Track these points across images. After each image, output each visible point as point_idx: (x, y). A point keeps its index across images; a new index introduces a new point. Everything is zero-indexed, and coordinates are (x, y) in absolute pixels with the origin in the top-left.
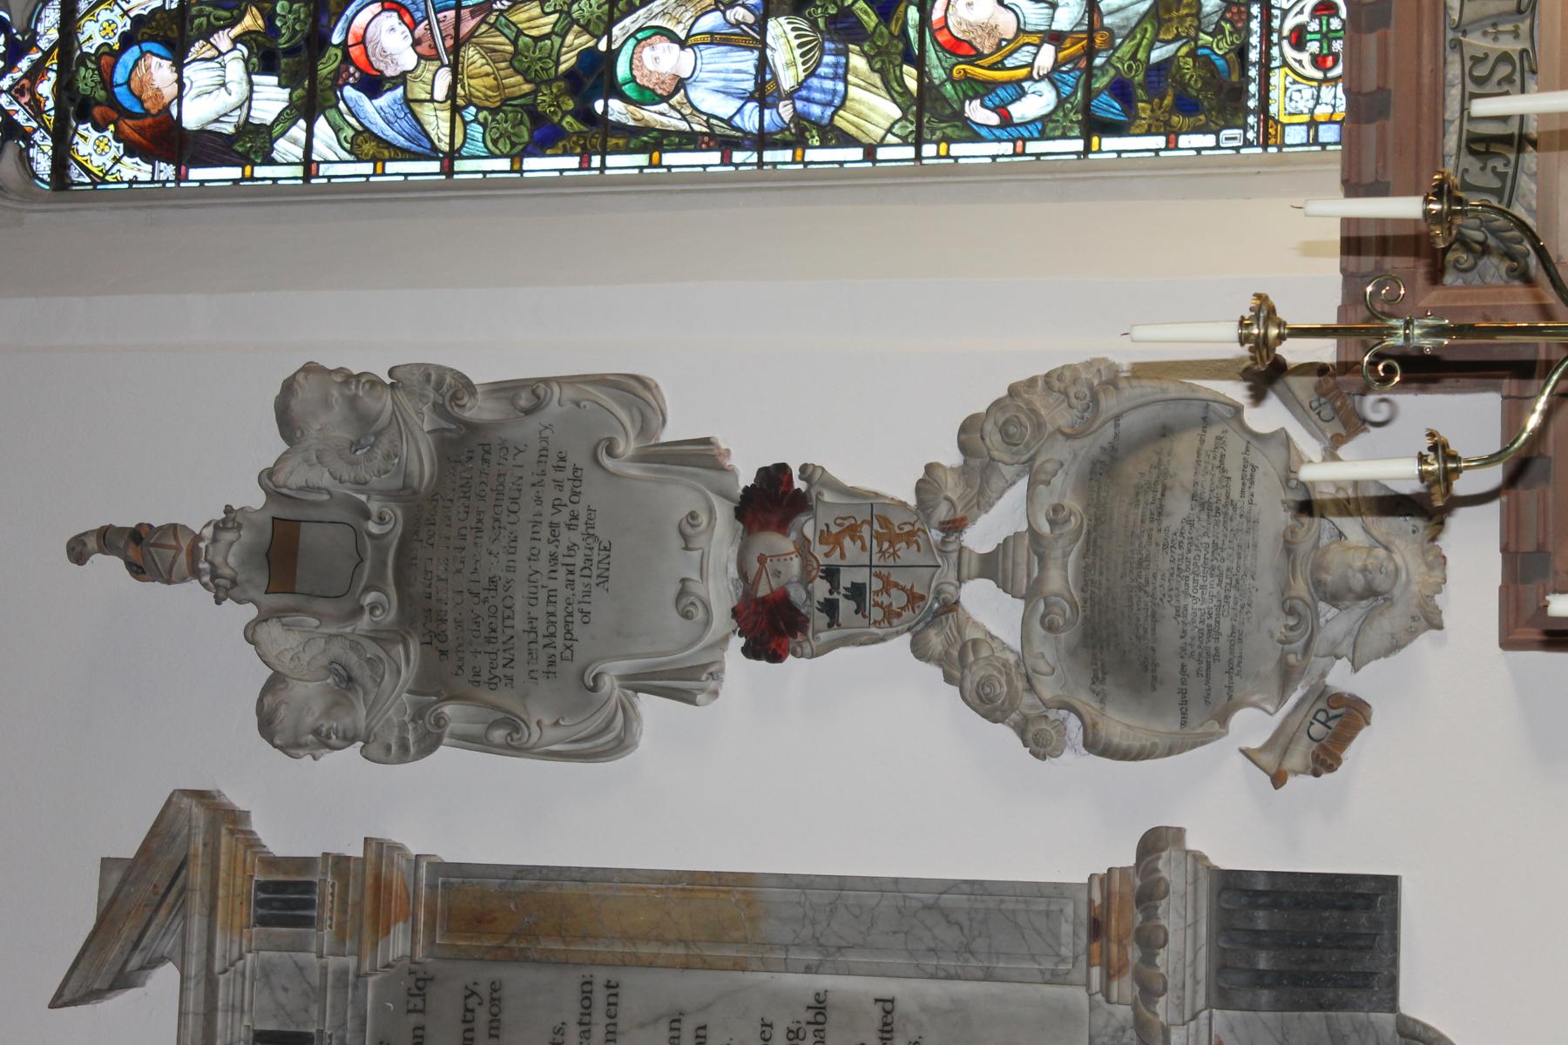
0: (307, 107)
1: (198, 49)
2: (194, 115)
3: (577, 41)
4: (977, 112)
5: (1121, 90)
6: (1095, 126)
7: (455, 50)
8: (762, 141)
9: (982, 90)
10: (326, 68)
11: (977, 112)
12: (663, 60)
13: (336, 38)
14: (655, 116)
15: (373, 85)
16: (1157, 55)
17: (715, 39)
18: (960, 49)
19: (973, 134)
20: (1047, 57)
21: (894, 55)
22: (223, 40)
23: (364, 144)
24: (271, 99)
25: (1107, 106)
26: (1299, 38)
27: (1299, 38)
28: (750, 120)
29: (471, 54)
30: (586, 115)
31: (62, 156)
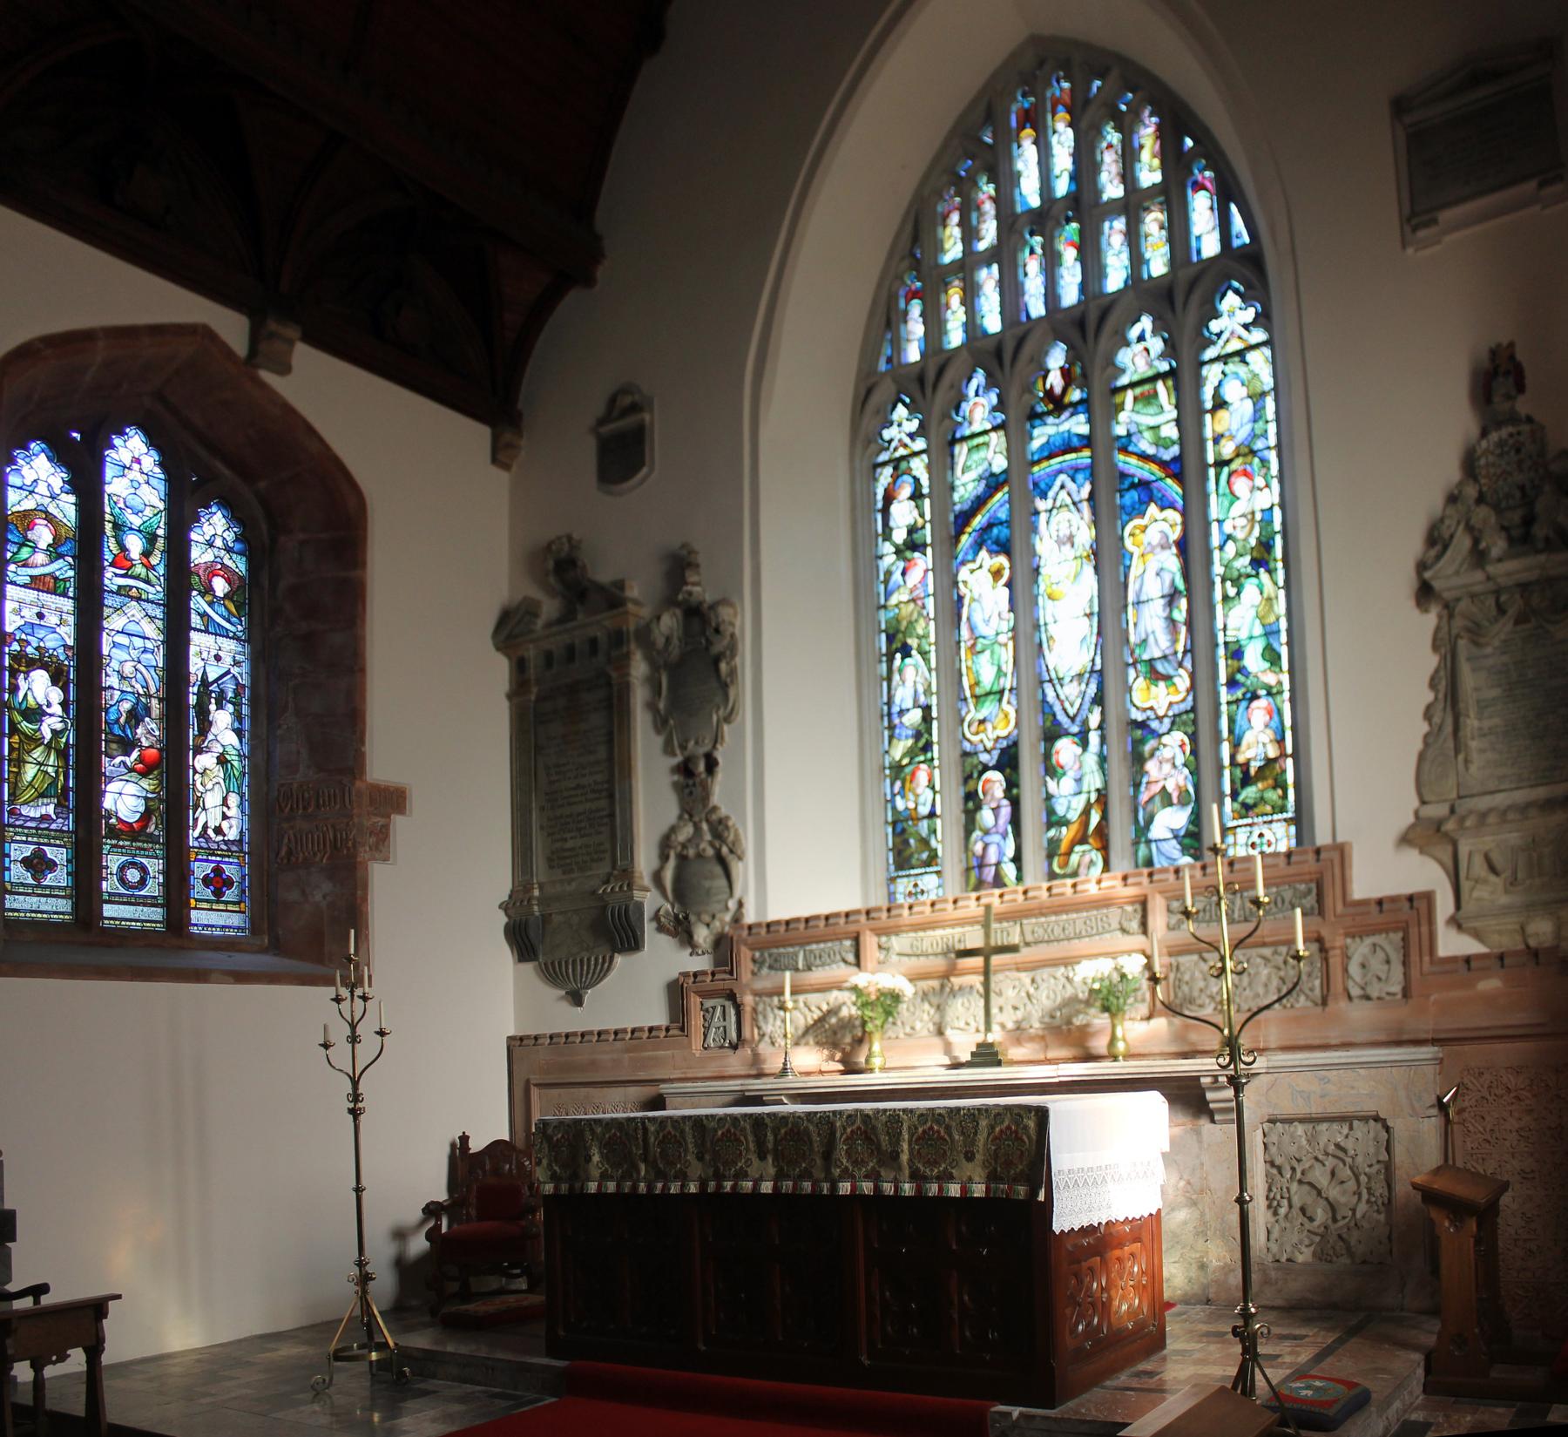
0: (899, 552)
1: (912, 503)
2: (894, 508)
3: (913, 642)
4: (898, 784)
5: (904, 831)
6: (894, 823)
7: (913, 600)
8: (890, 714)
9: (903, 787)
10: (908, 554)
11: (898, 784)
12: (910, 673)
13: (916, 554)
14: (896, 677)
15: (904, 573)
16: (912, 841)
17: (916, 692)
18: (913, 774)
19: (892, 785)
20: (911, 805)
21: (911, 753)
22: (916, 513)
23: (889, 573)
24: (900, 536)
25: (899, 829)
26: (916, 885)
27: (916, 885)
28: (895, 709)
29: (912, 605)
30: (897, 651)
31: (884, 464)
